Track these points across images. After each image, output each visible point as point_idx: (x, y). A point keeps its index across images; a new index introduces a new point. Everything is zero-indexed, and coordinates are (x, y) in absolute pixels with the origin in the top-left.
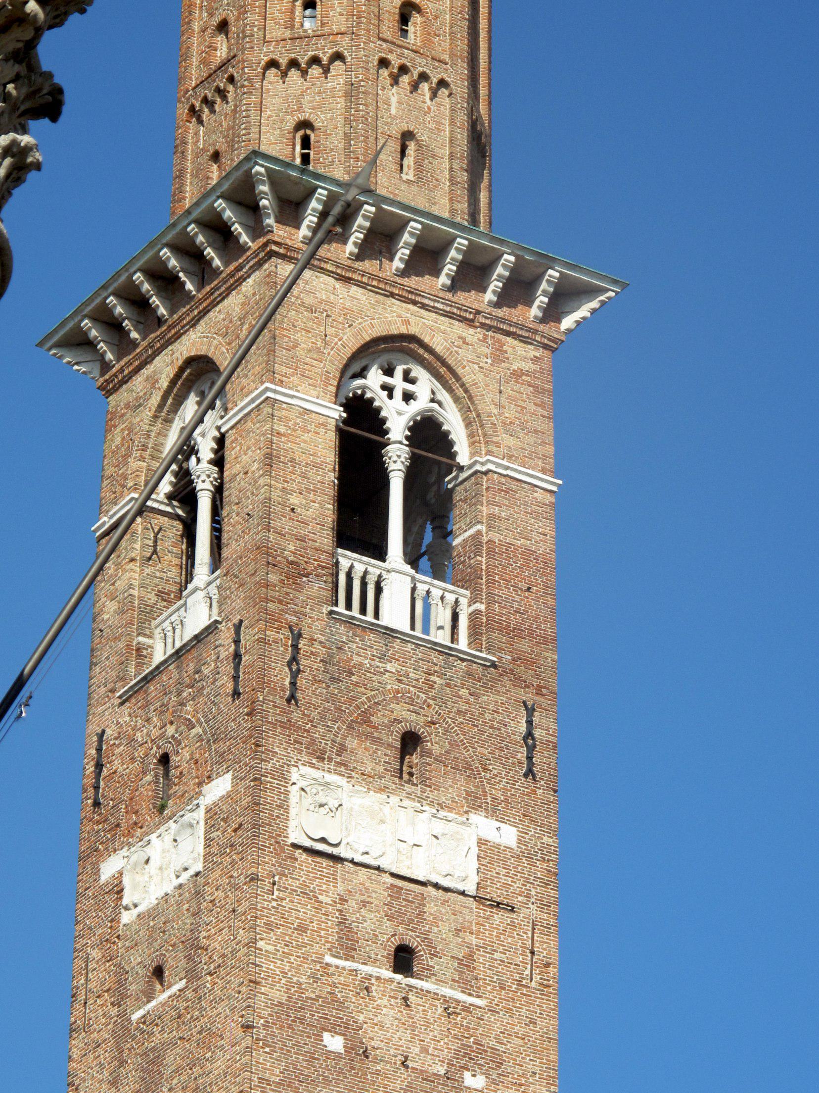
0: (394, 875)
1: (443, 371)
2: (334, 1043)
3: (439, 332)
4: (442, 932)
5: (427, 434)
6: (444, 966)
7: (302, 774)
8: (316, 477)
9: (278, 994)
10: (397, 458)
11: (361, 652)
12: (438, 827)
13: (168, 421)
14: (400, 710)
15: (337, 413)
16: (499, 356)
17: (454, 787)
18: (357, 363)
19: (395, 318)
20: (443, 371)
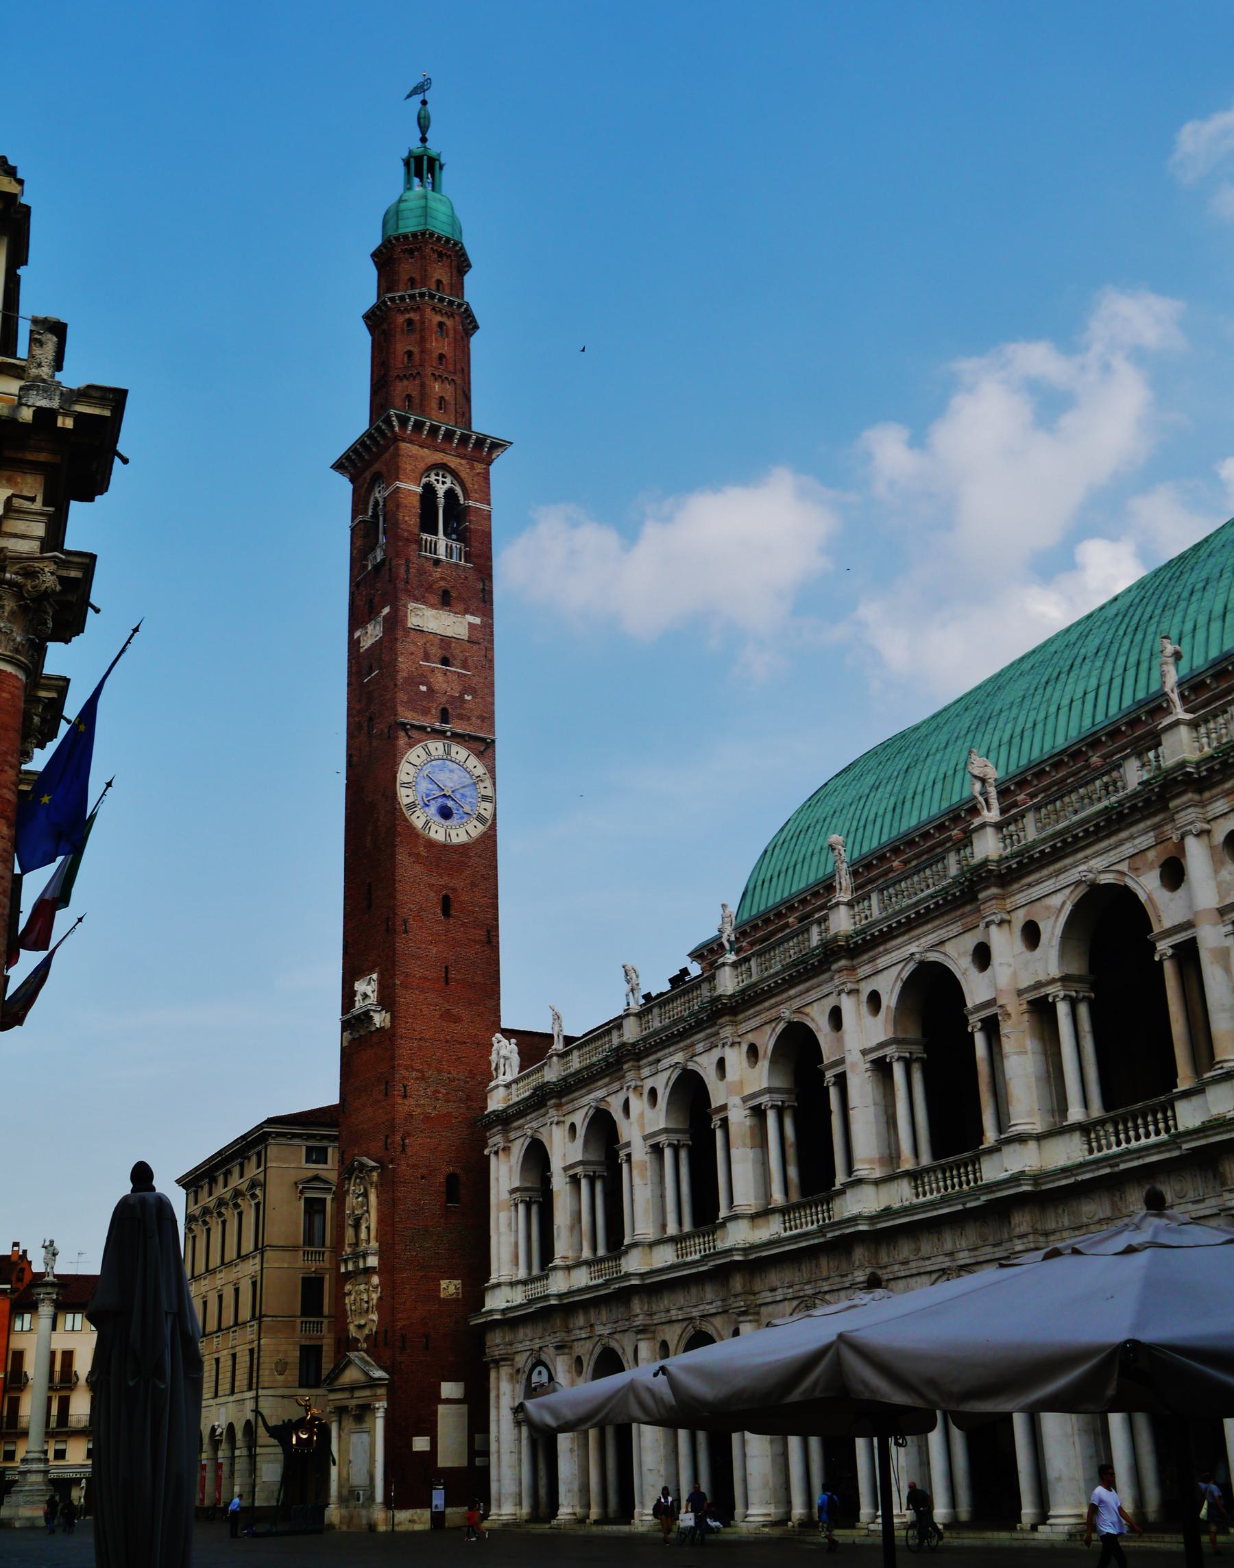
1: (455, 474)
2: (423, 688)
3: (453, 462)
4: (457, 652)
5: (450, 493)
6: (457, 662)
7: (411, 605)
8: (414, 511)
9: (405, 675)
10: (441, 502)
11: (429, 566)
12: (455, 619)
14: (442, 583)
15: (419, 490)
16: (472, 468)
17: (461, 607)
18: (429, 469)
19: (438, 457)
20: (455, 474)
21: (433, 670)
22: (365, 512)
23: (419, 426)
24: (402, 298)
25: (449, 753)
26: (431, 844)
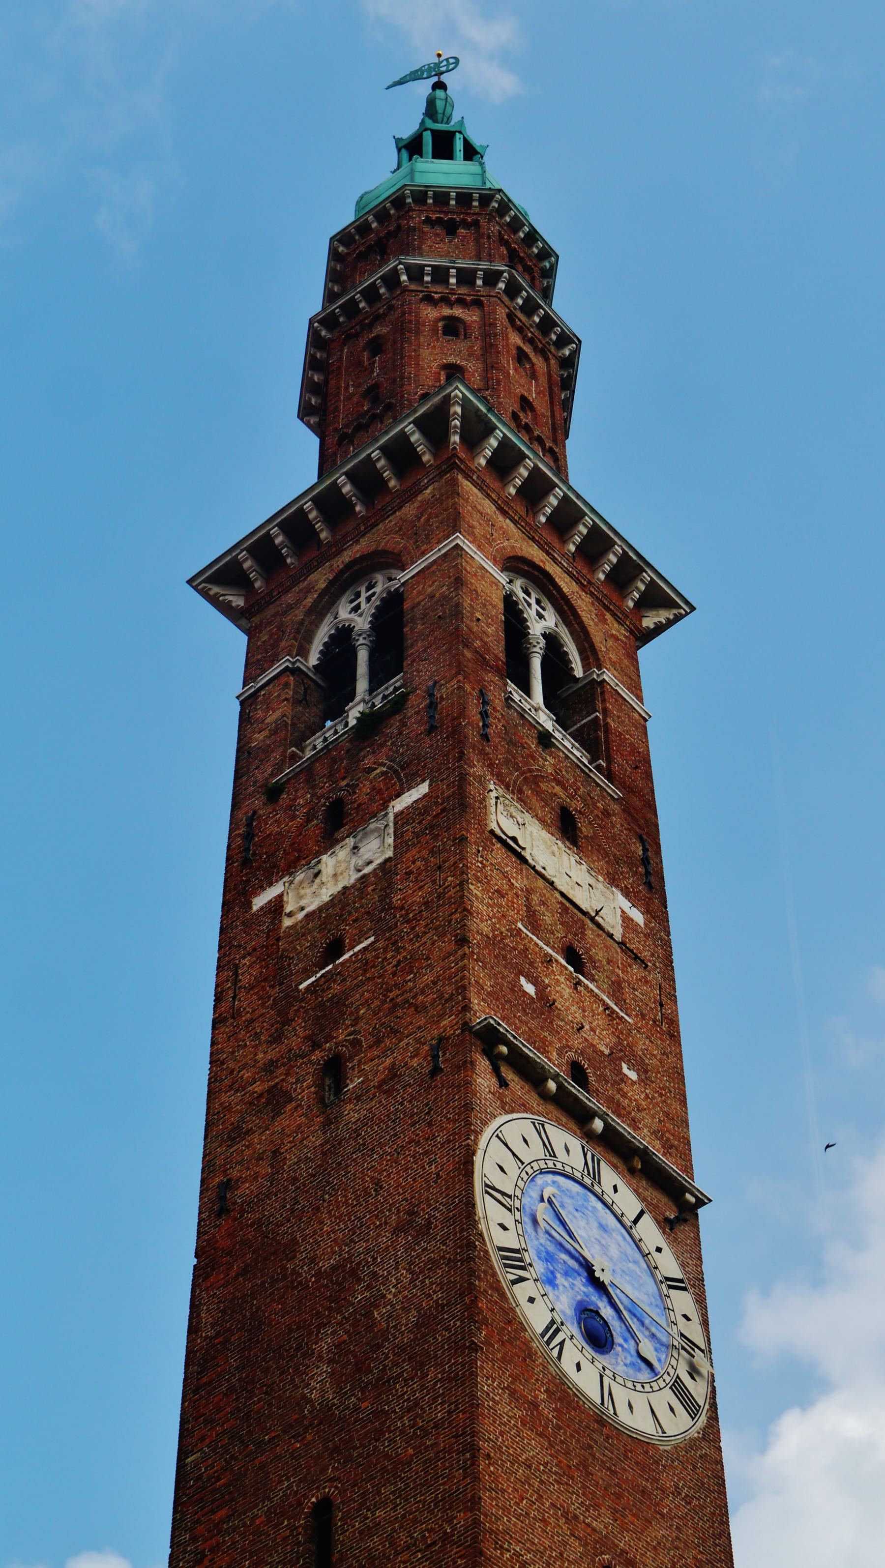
0: (563, 894)
2: (530, 989)
4: (600, 955)
7: (494, 790)
13: (321, 616)
21: (550, 961)
22: (303, 652)
23: (505, 461)
24: (440, 275)
25: (596, 1176)
26: (565, 1395)
